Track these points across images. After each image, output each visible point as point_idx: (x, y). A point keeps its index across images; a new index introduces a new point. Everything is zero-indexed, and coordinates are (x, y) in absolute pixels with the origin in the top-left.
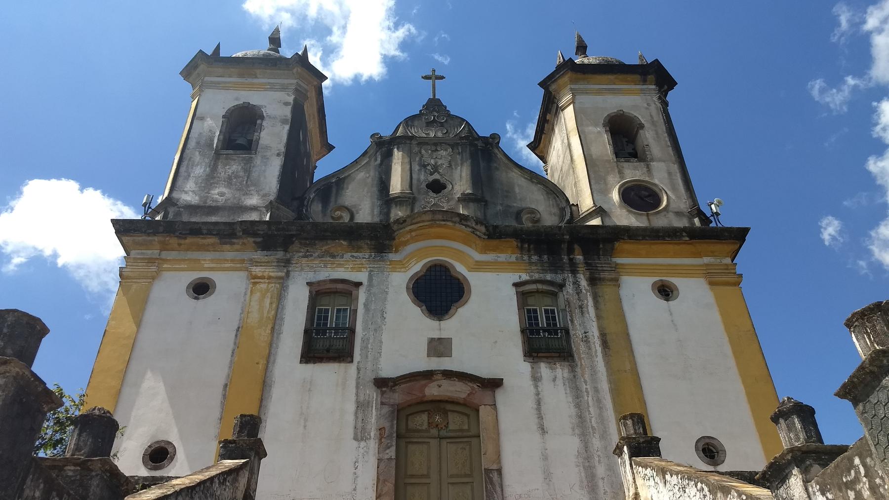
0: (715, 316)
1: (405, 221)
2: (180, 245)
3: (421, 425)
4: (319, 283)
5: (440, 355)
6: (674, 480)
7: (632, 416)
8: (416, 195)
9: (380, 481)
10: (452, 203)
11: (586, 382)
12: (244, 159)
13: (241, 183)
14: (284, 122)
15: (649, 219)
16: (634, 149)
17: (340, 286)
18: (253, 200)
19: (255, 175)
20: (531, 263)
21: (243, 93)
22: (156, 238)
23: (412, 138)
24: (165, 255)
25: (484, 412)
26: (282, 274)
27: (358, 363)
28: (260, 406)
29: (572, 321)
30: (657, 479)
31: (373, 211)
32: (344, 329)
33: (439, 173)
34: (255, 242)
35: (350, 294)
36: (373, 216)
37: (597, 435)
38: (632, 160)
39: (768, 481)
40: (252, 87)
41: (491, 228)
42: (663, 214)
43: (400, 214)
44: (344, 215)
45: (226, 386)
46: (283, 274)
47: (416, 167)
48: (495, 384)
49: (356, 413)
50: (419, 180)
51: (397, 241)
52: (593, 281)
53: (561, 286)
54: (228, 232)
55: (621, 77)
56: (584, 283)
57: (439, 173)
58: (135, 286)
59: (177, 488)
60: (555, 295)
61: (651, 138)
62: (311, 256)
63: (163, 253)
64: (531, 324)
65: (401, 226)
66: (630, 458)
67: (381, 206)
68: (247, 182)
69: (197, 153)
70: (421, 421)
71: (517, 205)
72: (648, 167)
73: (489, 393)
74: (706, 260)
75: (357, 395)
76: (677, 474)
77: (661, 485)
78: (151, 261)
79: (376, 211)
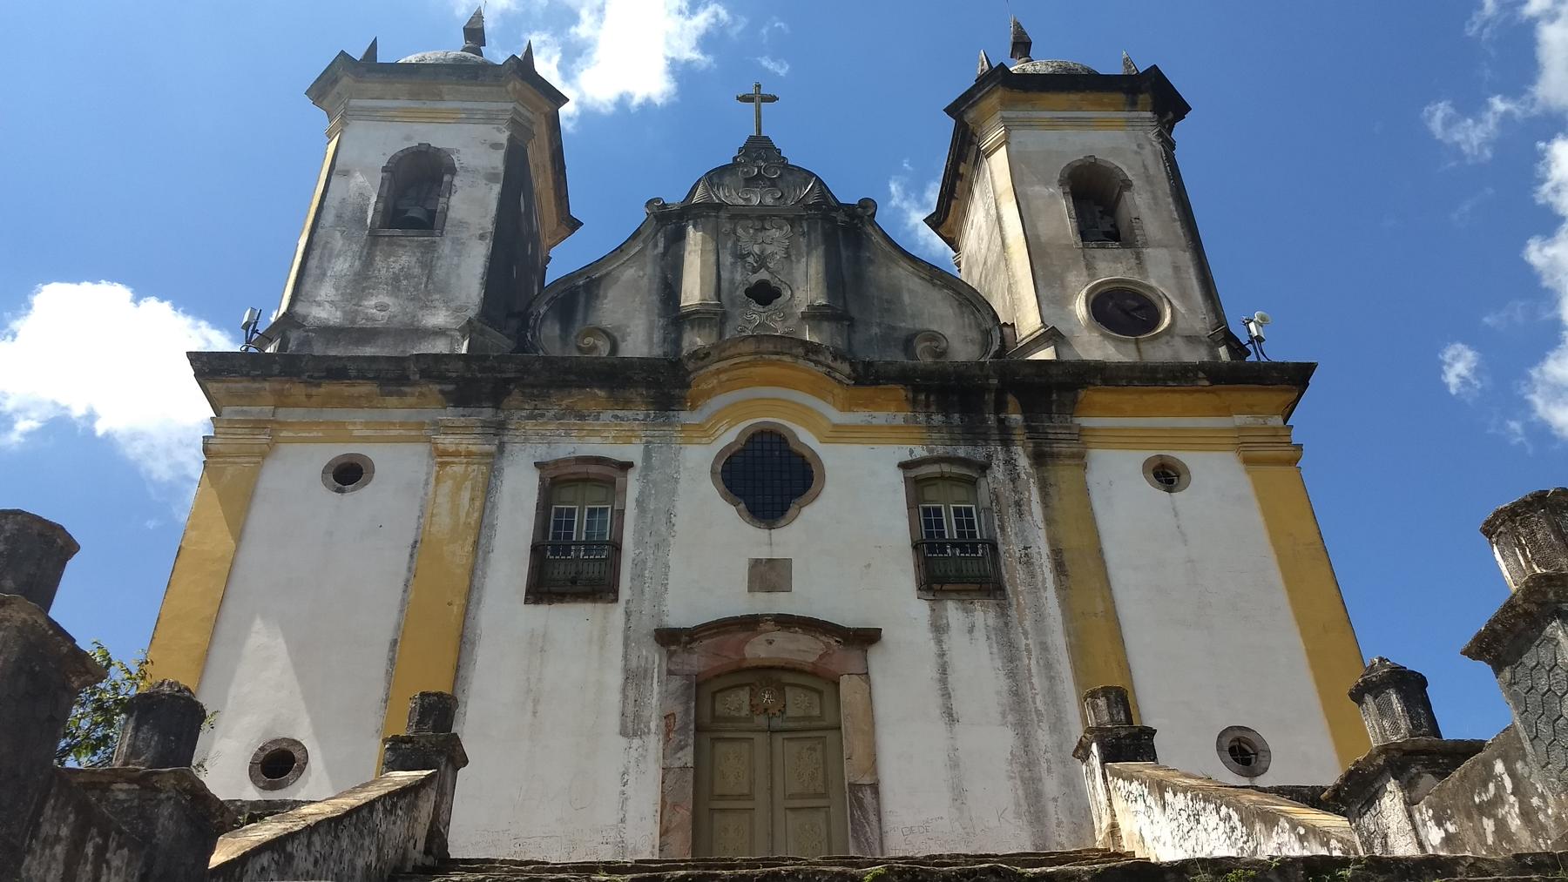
0: (1255, 518)
1: (707, 355)
2: (309, 396)
3: (739, 709)
4: (557, 462)
5: (771, 589)
6: (1180, 801)
7: (1106, 691)
8: (727, 308)
9: (667, 805)
10: (792, 322)
11: (1025, 634)
12: (421, 245)
13: (416, 288)
14: (491, 178)
15: (1139, 350)
16: (1114, 225)
17: (594, 469)
18: (439, 318)
19: (440, 273)
20: (930, 428)
21: (417, 126)
22: (267, 385)
23: (721, 206)
24: (283, 414)
26: (493, 448)
27: (628, 602)
28: (456, 678)
29: (1002, 529)
30: (1150, 800)
31: (650, 338)
32: (601, 544)
33: (768, 269)
34: (442, 392)
35: (612, 482)
36: (651, 347)
37: (1045, 726)
38: (1110, 244)
39: (1344, 803)
40: (433, 117)
41: (860, 368)
42: (1164, 339)
43: (699, 341)
44: (600, 343)
45: (395, 642)
46: (493, 448)
47: (727, 259)
48: (867, 638)
49: (624, 690)
50: (732, 281)
51: (693, 391)
52: (1040, 459)
53: (984, 468)
54: (395, 374)
55: (1091, 96)
56: (1023, 462)
57: (768, 269)
58: (230, 470)
59: (311, 821)
60: (972, 483)
61: (1144, 205)
62: (542, 416)
63: (280, 410)
64: (930, 535)
65: (700, 363)
66: (1103, 764)
67: (665, 328)
68: (428, 286)
69: (338, 234)
70: (738, 702)
71: (907, 325)
73: (854, 655)
74: (1239, 420)
75: (625, 657)
76: (1185, 790)
77: (1157, 810)
78: (258, 425)
79: (657, 336)
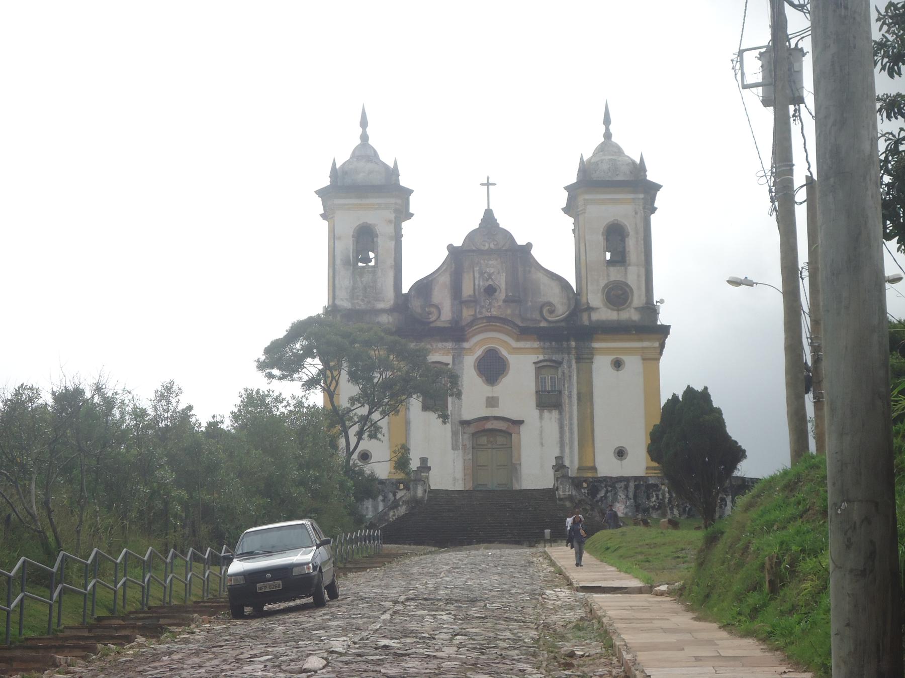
20: (544, 348)
47: (477, 275)
48: (521, 422)
50: (479, 285)
52: (579, 359)
53: (560, 363)
56: (574, 362)
60: (557, 368)
61: (632, 244)
70: (483, 440)
74: (646, 344)
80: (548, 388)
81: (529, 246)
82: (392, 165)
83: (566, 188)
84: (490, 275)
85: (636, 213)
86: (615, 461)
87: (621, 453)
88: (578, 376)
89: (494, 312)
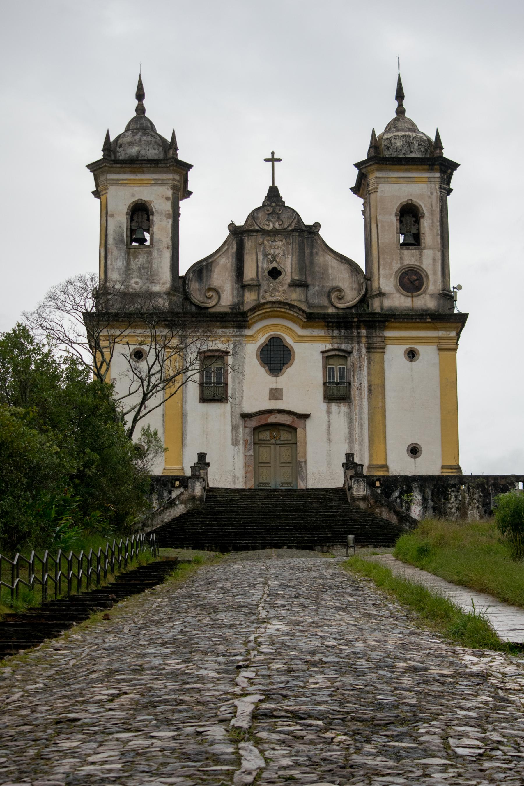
0: (436, 372)
3: (266, 437)
5: (276, 399)
9: (246, 466)
11: (356, 414)
20: (333, 337)
25: (299, 431)
29: (354, 376)
31: (233, 294)
32: (221, 383)
36: (233, 297)
37: (357, 443)
40: (141, 183)
42: (422, 296)
45: (163, 415)
47: (260, 257)
48: (306, 417)
49: (232, 431)
50: (262, 268)
52: (369, 349)
53: (350, 353)
56: (364, 351)
57: (276, 261)
60: (346, 358)
70: (266, 435)
72: (421, 255)
73: (302, 421)
74: (441, 333)
75: (232, 421)
80: (337, 379)
81: (317, 225)
82: (169, 139)
83: (357, 165)
84: (274, 257)
85: (432, 193)
86: (409, 459)
87: (414, 451)
88: (369, 368)
89: (278, 297)
